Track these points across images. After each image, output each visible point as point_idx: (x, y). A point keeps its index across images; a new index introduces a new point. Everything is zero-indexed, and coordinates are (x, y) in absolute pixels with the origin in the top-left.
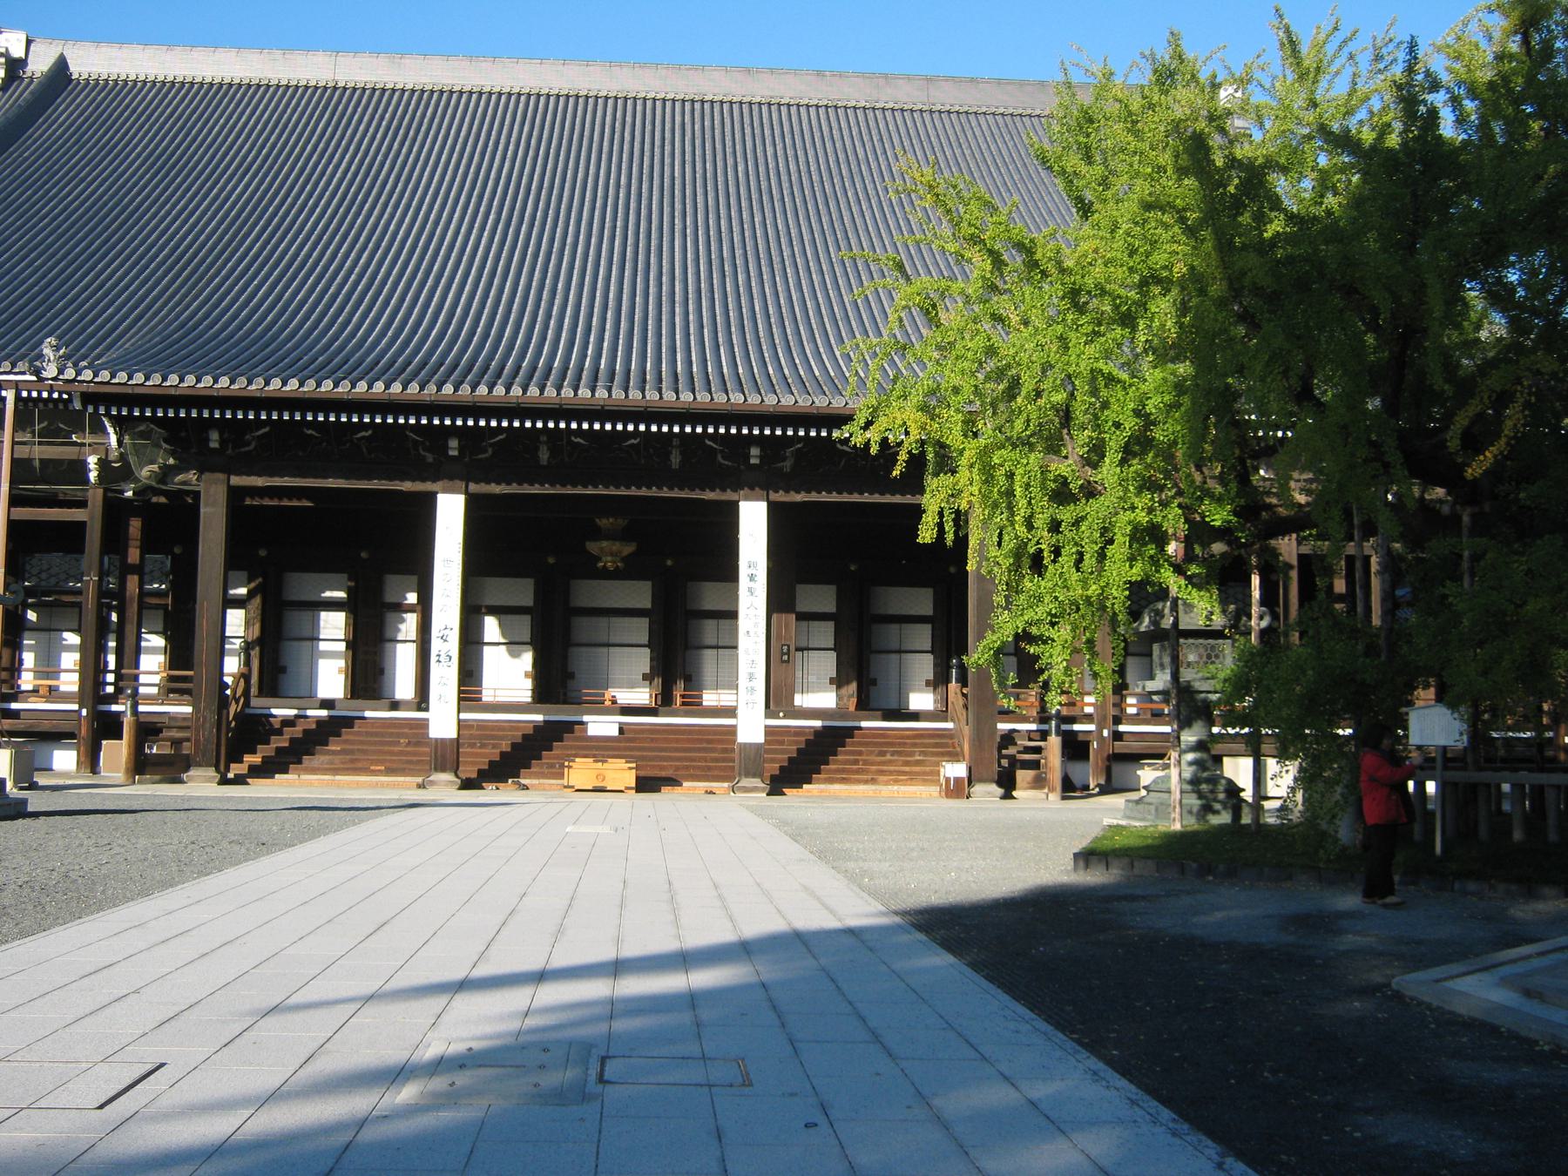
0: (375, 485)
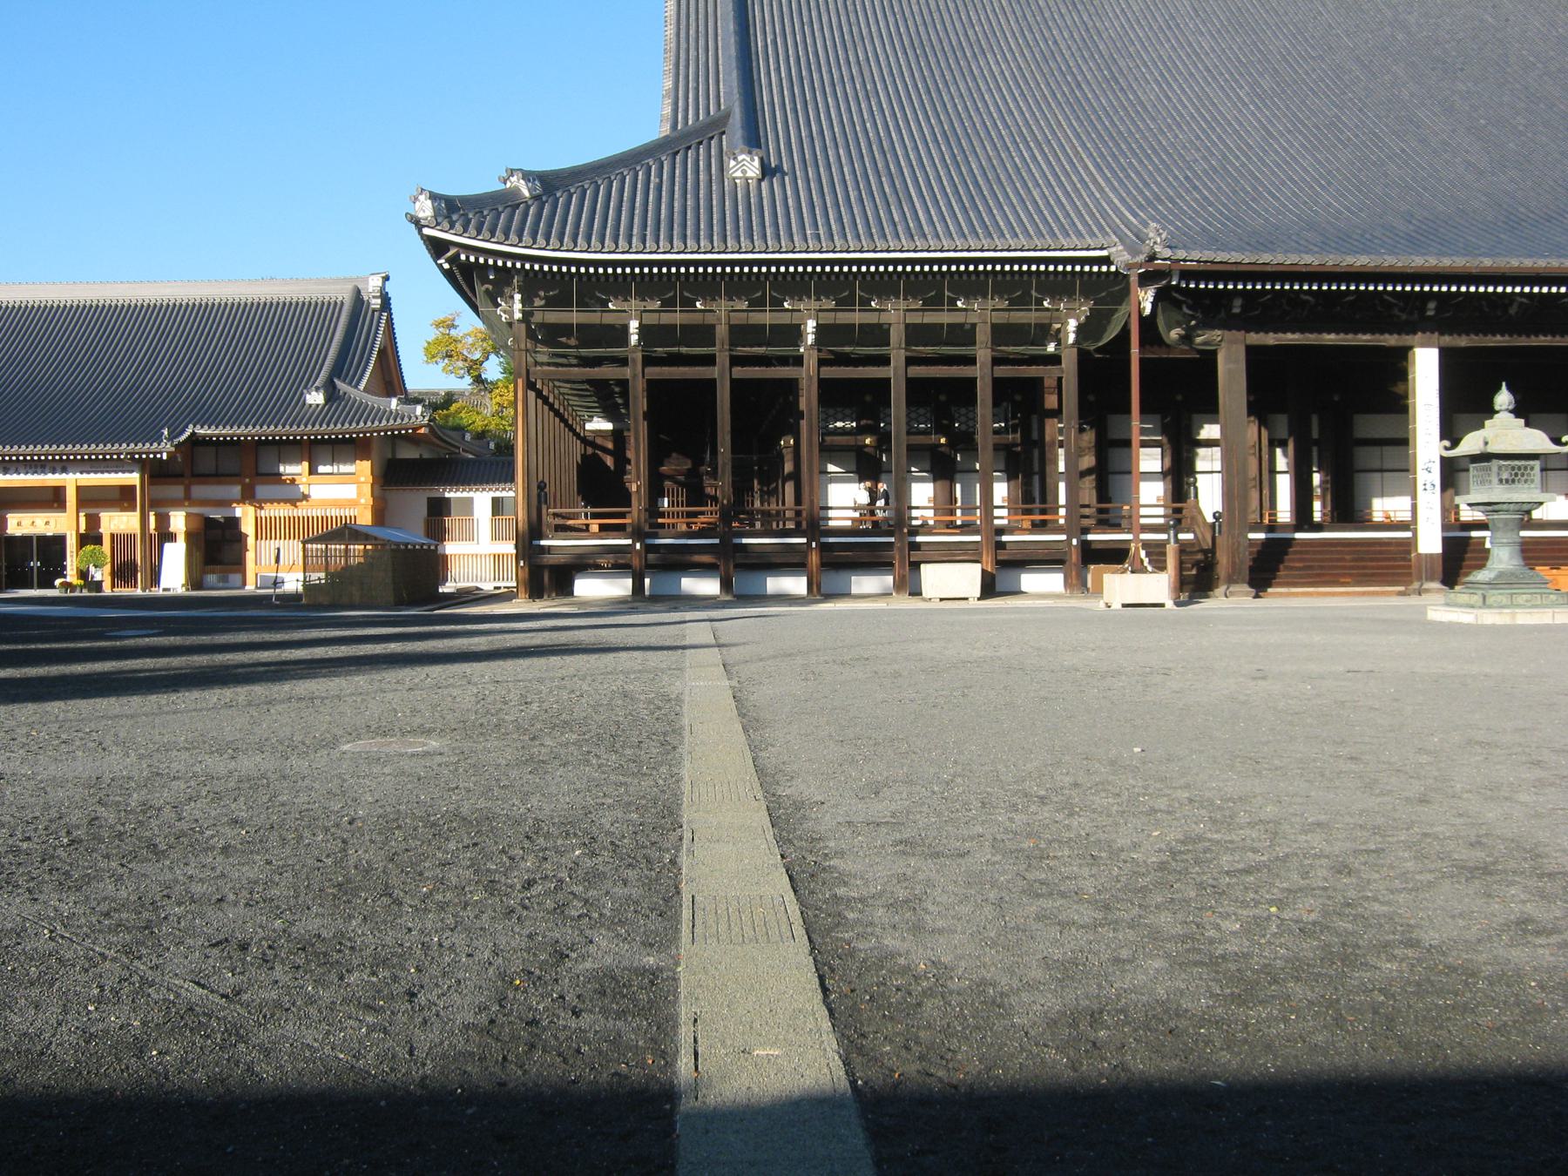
0: (1364, 339)
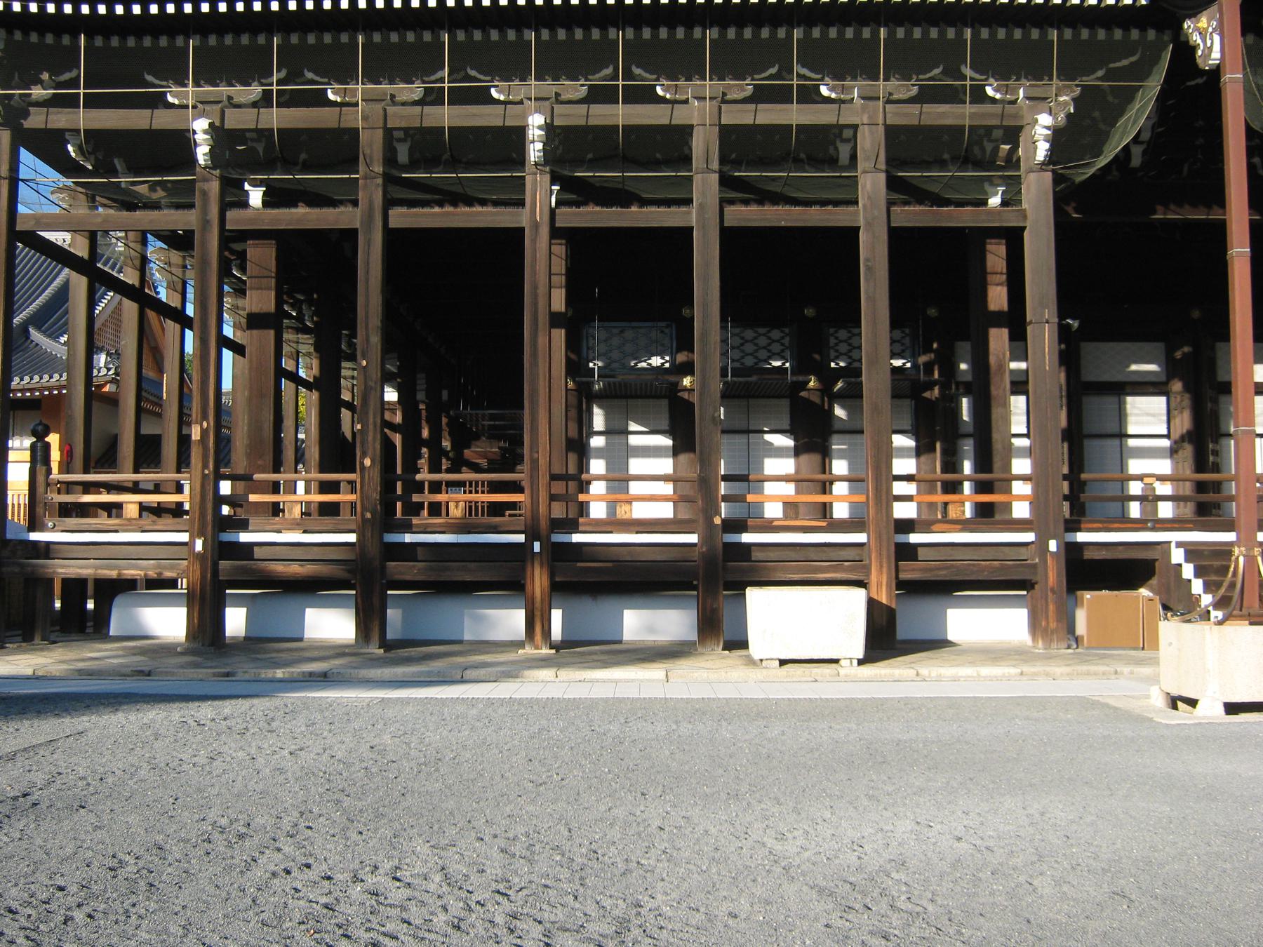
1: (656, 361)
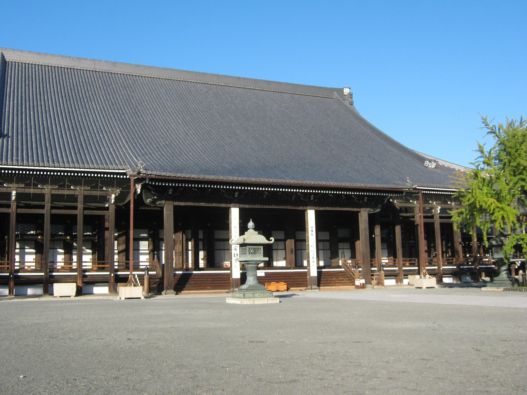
0: (214, 205)
1: (32, 232)
